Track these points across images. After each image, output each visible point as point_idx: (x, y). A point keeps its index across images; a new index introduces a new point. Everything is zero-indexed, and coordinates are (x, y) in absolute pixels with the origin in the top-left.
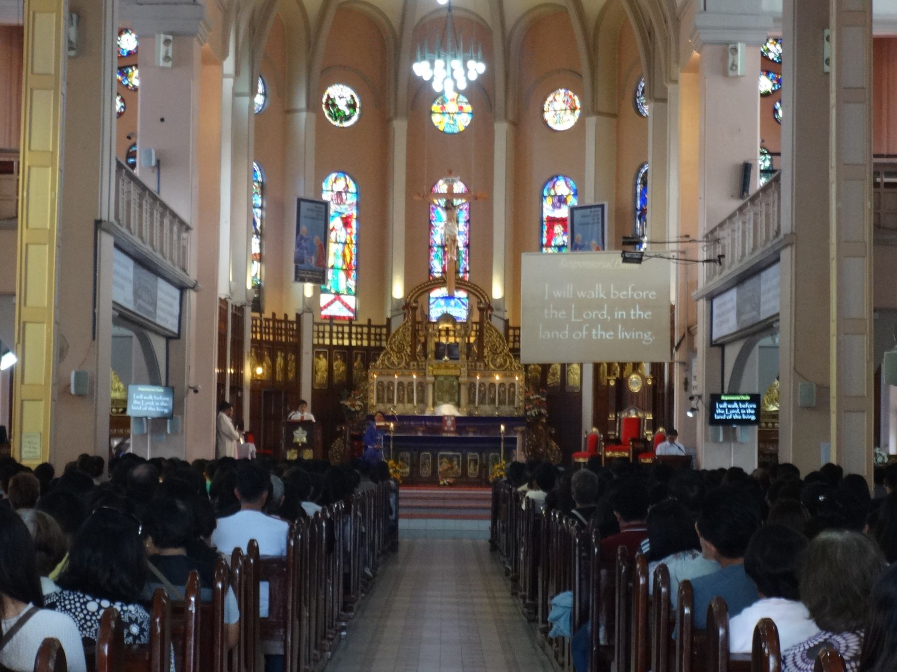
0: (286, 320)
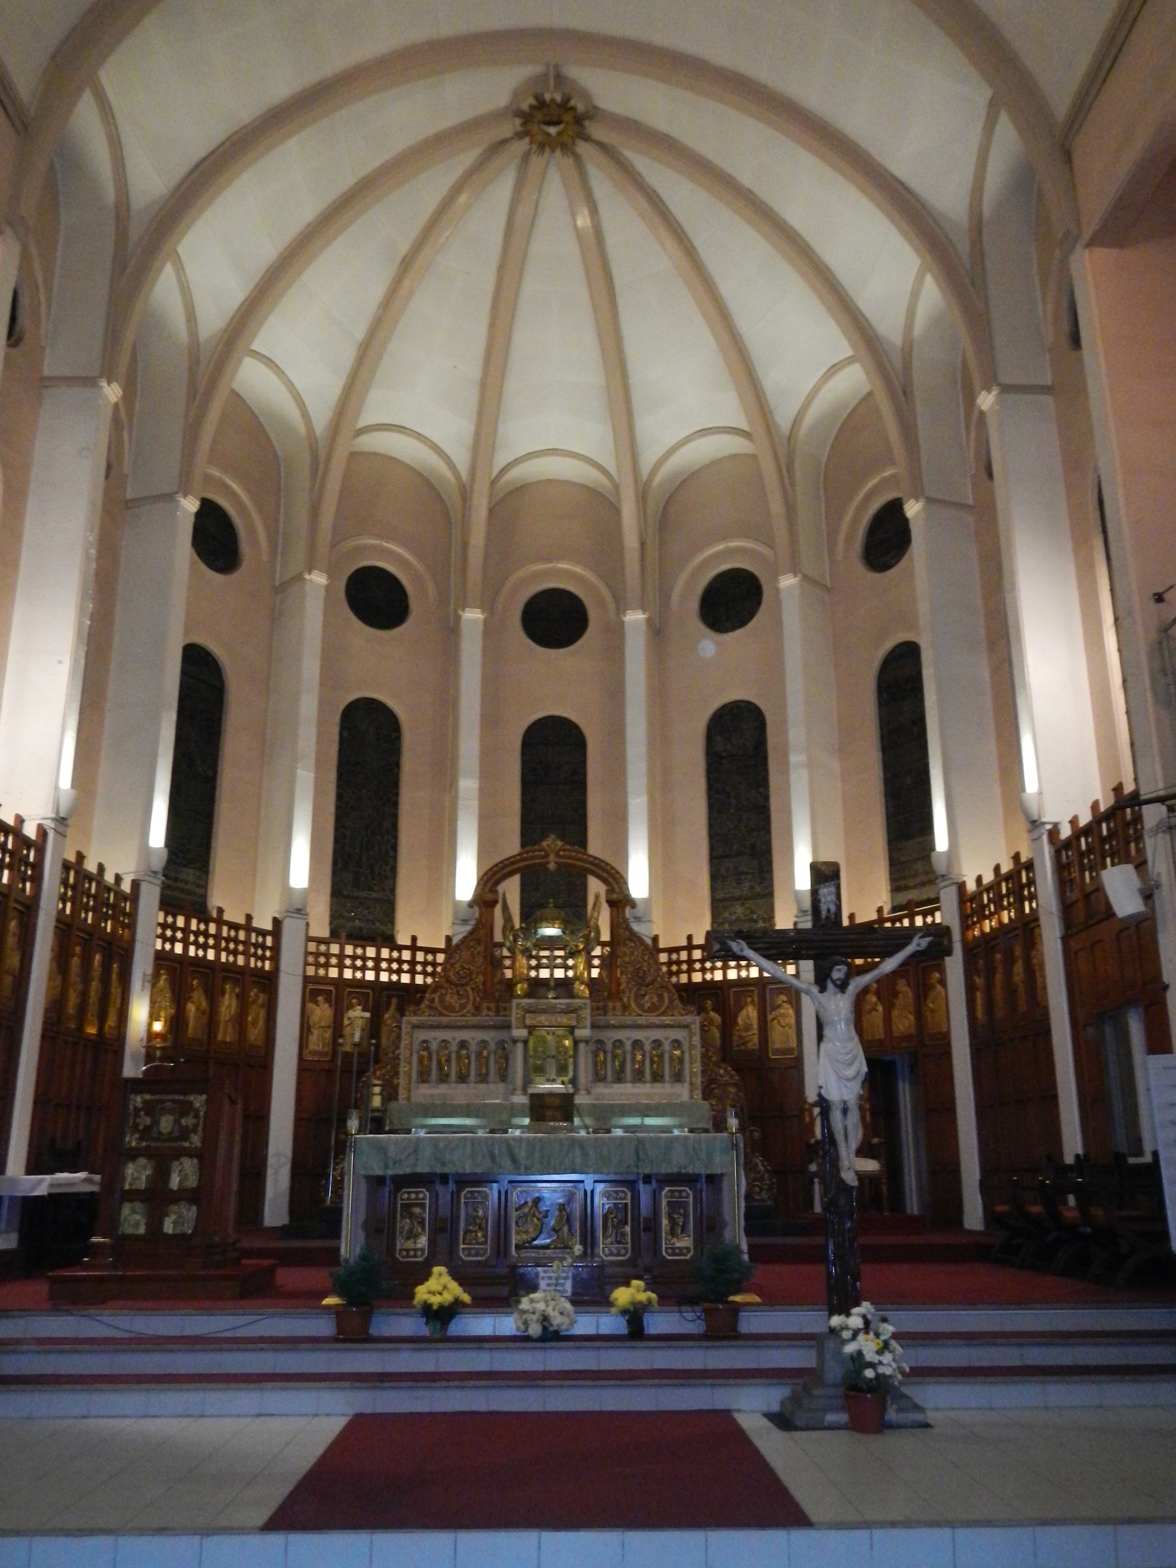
0: (248, 927)
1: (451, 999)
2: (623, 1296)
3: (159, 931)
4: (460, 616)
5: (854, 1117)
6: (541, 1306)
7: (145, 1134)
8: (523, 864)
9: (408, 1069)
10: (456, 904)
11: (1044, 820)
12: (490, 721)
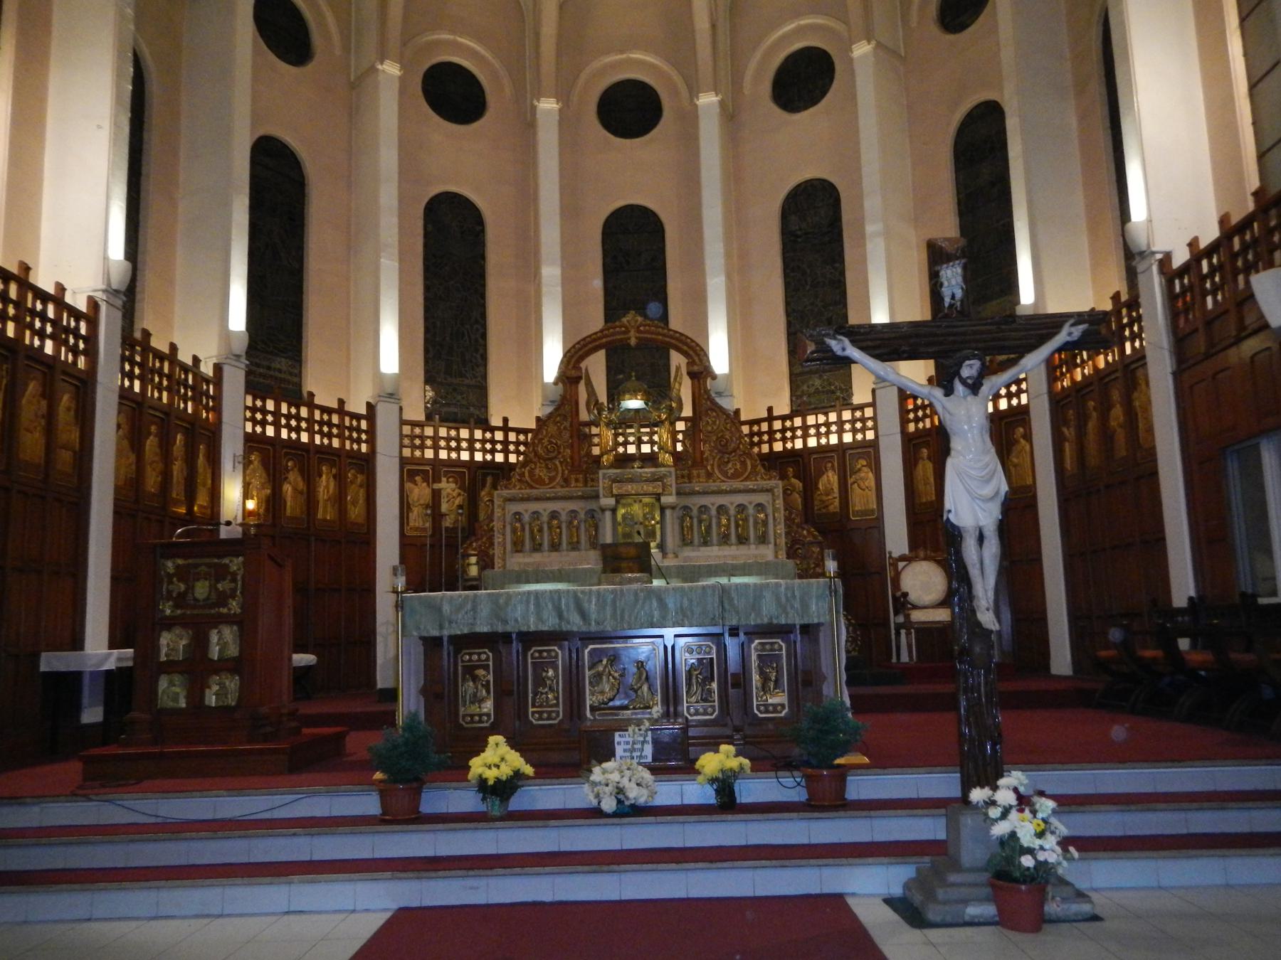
0: (341, 410)
1: (541, 472)
2: (711, 763)
3: (248, 414)
4: (536, 107)
5: (992, 547)
6: (615, 777)
7: (180, 600)
8: (604, 340)
9: (502, 539)
10: (544, 386)
11: (1154, 249)
12: (570, 212)
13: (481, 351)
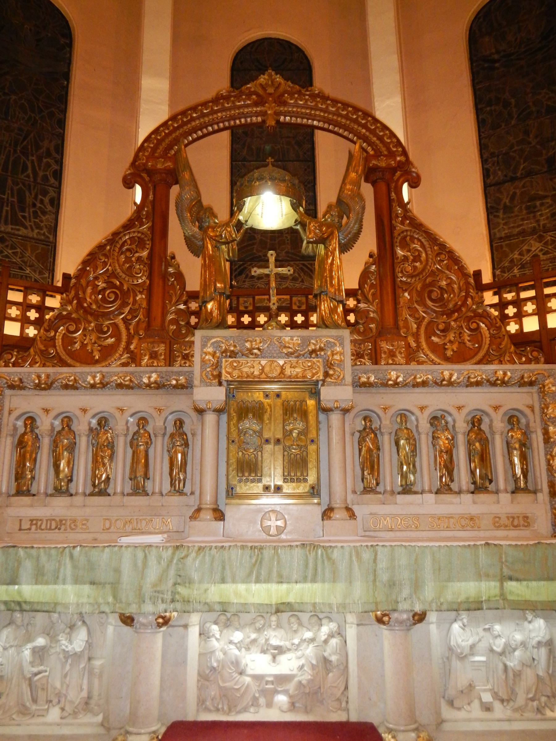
13: (52, 194)
